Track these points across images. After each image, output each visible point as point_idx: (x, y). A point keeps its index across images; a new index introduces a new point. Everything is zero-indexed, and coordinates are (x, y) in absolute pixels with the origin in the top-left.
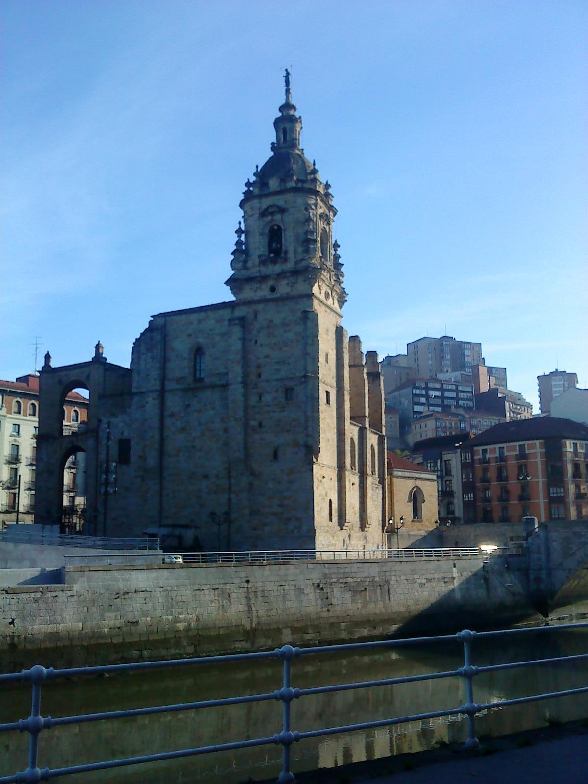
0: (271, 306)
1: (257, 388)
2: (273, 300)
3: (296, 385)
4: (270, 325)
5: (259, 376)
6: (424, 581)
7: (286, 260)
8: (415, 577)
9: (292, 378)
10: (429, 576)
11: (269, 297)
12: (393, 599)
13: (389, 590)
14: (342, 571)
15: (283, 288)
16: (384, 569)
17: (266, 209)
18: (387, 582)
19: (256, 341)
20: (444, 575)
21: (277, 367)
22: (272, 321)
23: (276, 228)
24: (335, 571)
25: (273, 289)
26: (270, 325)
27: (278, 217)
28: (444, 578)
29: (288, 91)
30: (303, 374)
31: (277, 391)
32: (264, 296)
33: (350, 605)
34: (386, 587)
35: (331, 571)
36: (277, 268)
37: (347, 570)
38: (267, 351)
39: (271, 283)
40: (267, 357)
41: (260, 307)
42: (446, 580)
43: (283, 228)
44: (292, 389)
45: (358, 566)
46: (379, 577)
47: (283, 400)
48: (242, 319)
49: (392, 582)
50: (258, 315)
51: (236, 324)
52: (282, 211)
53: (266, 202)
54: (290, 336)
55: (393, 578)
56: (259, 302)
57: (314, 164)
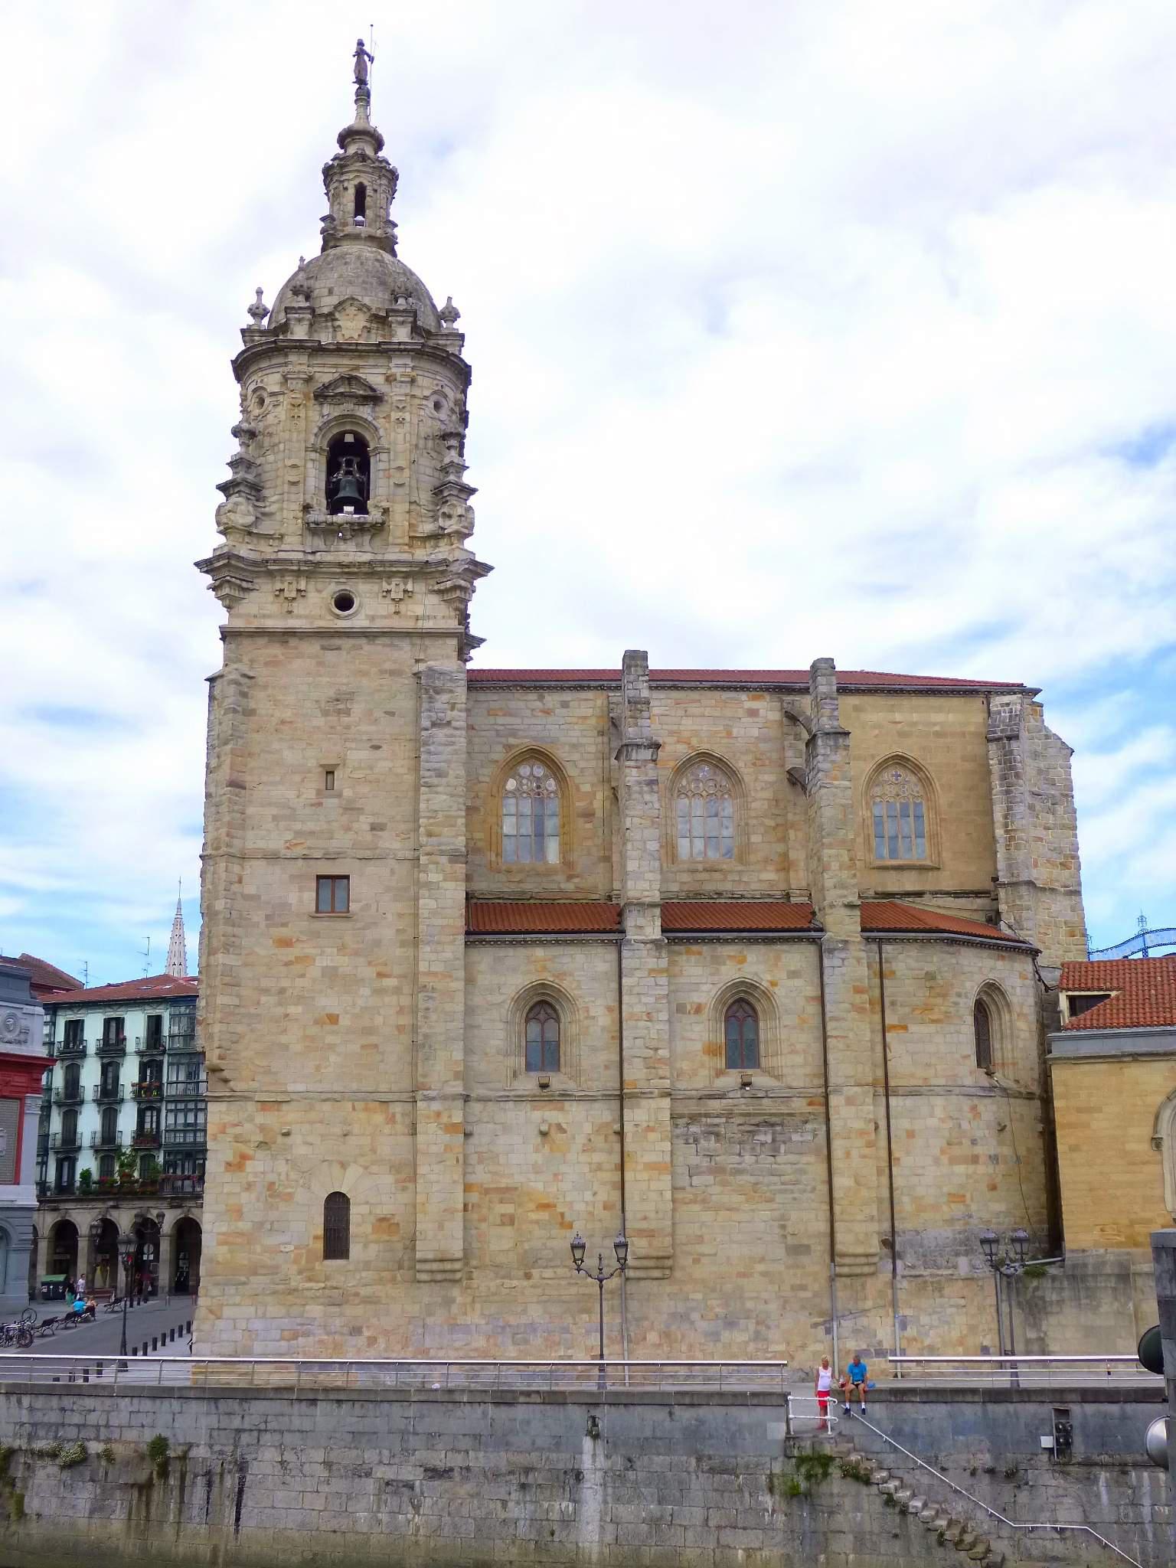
6: (410, 1473)
8: (370, 1456)
10: (439, 1459)
12: (253, 1523)
13: (241, 1492)
14: (76, 1419)
16: (236, 1423)
18: (242, 1467)
20: (522, 1460)
24: (53, 1417)
28: (528, 1470)
29: (363, 96)
33: (82, 1523)
34: (230, 1482)
35: (39, 1417)
37: (92, 1419)
42: (531, 1479)
45: (135, 1408)
46: (211, 1446)
49: (254, 1468)
55: (270, 1455)
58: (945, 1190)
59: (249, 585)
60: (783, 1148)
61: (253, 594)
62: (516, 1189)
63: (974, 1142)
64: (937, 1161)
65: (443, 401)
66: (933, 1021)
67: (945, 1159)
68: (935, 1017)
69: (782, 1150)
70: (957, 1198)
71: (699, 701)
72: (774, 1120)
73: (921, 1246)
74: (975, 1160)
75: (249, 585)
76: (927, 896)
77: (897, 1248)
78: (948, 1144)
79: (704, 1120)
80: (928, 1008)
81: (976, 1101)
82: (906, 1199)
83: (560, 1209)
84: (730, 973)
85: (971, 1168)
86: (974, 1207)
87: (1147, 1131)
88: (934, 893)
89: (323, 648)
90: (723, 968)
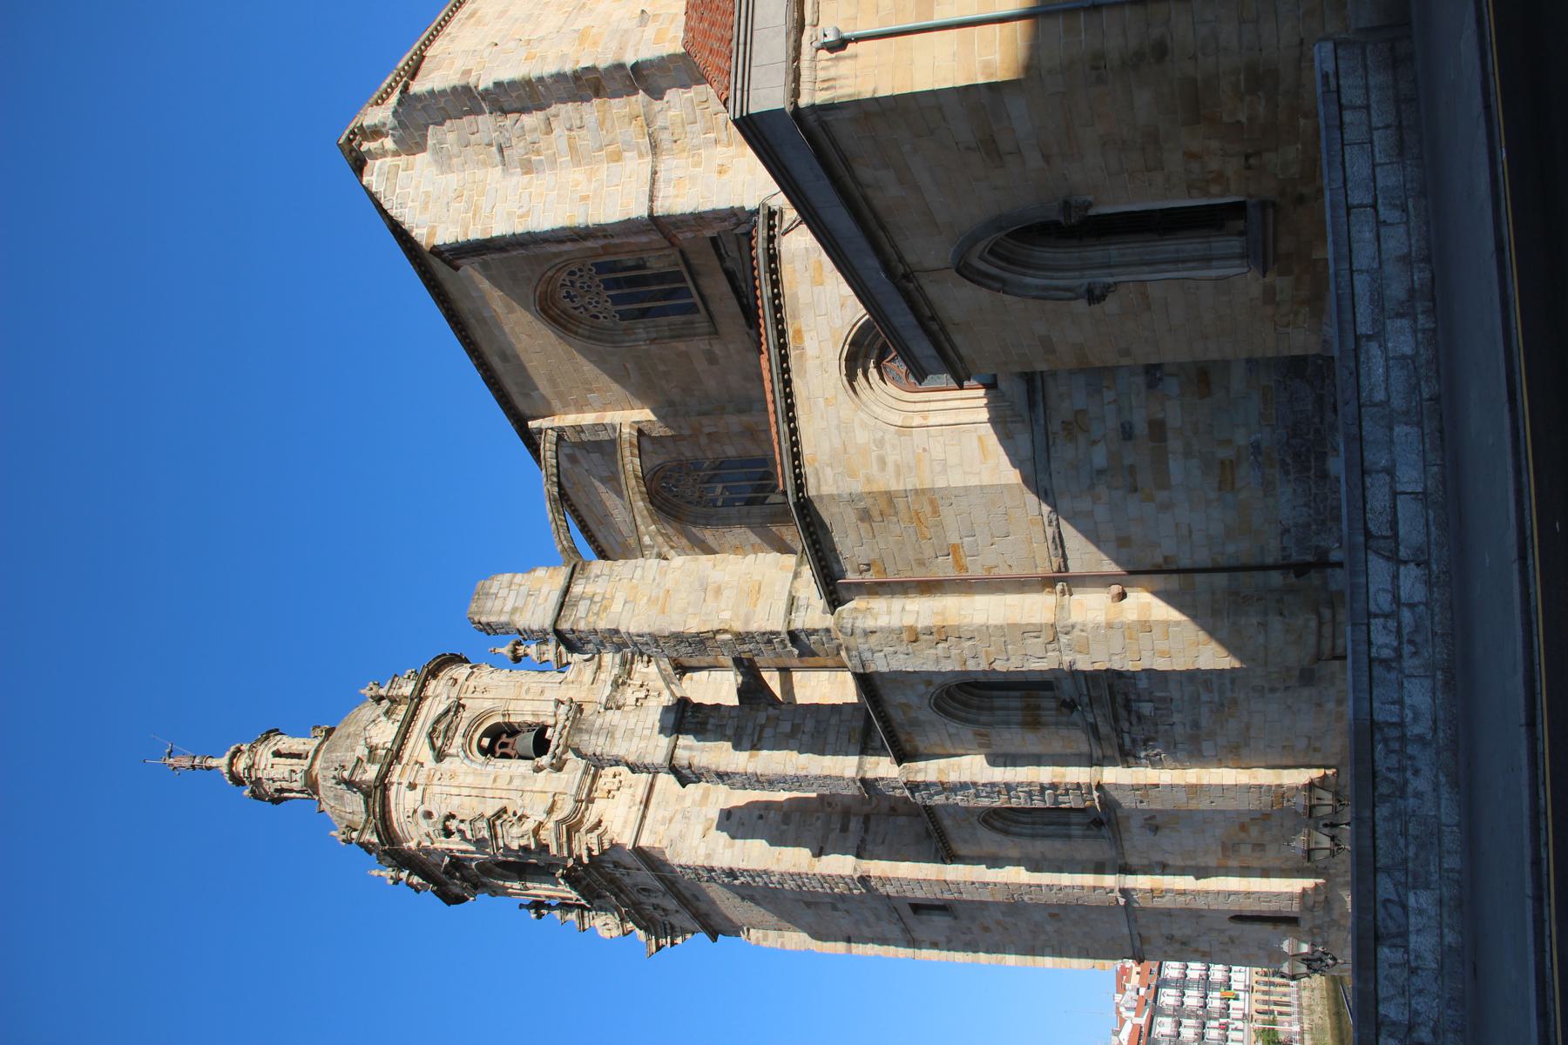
58: (1213, 495)
59: (668, 926)
60: (1158, 694)
61: (673, 922)
62: (1223, 842)
63: (1127, 433)
64: (1166, 507)
65: (421, 810)
66: (936, 512)
67: (1162, 496)
68: (928, 509)
69: (1163, 694)
70: (1226, 474)
71: (586, 505)
72: (1119, 699)
73: (1309, 525)
74: (1158, 430)
75: (668, 926)
76: (729, 264)
77: (1309, 558)
78: (1135, 490)
79: (1127, 748)
80: (917, 517)
81: (1056, 426)
82: (1231, 549)
83: (1248, 820)
84: (927, 714)
85: (1174, 444)
86: (1241, 438)
87: (1081, 306)
88: (721, 257)
89: (698, 900)
90: (922, 718)
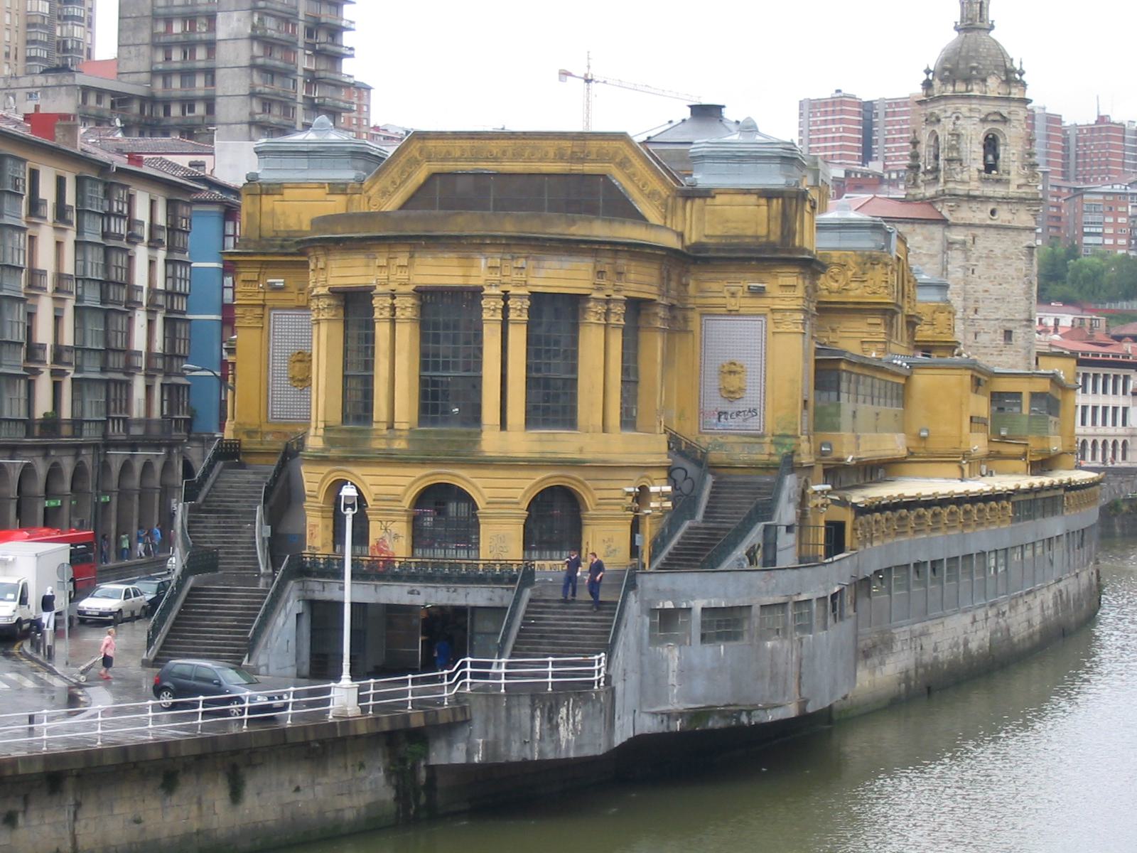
0: (992, 232)
1: (974, 325)
2: (989, 226)
3: (1015, 328)
4: (989, 255)
5: (976, 311)
7: (1008, 182)
9: (1012, 320)
11: (989, 222)
15: (1004, 216)
17: (989, 114)
19: (973, 270)
21: (996, 304)
22: (992, 251)
23: (991, 136)
25: (993, 212)
26: (989, 255)
27: (1000, 127)
30: (1025, 316)
31: (995, 332)
32: (984, 219)
36: (999, 191)
38: (988, 286)
39: (991, 206)
40: (986, 291)
41: (979, 232)
43: (1001, 141)
44: (1011, 332)
47: (1002, 343)
48: (964, 243)
50: (976, 239)
51: (956, 249)
52: (1005, 120)
53: (987, 108)
54: (1011, 271)
56: (980, 226)
57: (1021, 63)
